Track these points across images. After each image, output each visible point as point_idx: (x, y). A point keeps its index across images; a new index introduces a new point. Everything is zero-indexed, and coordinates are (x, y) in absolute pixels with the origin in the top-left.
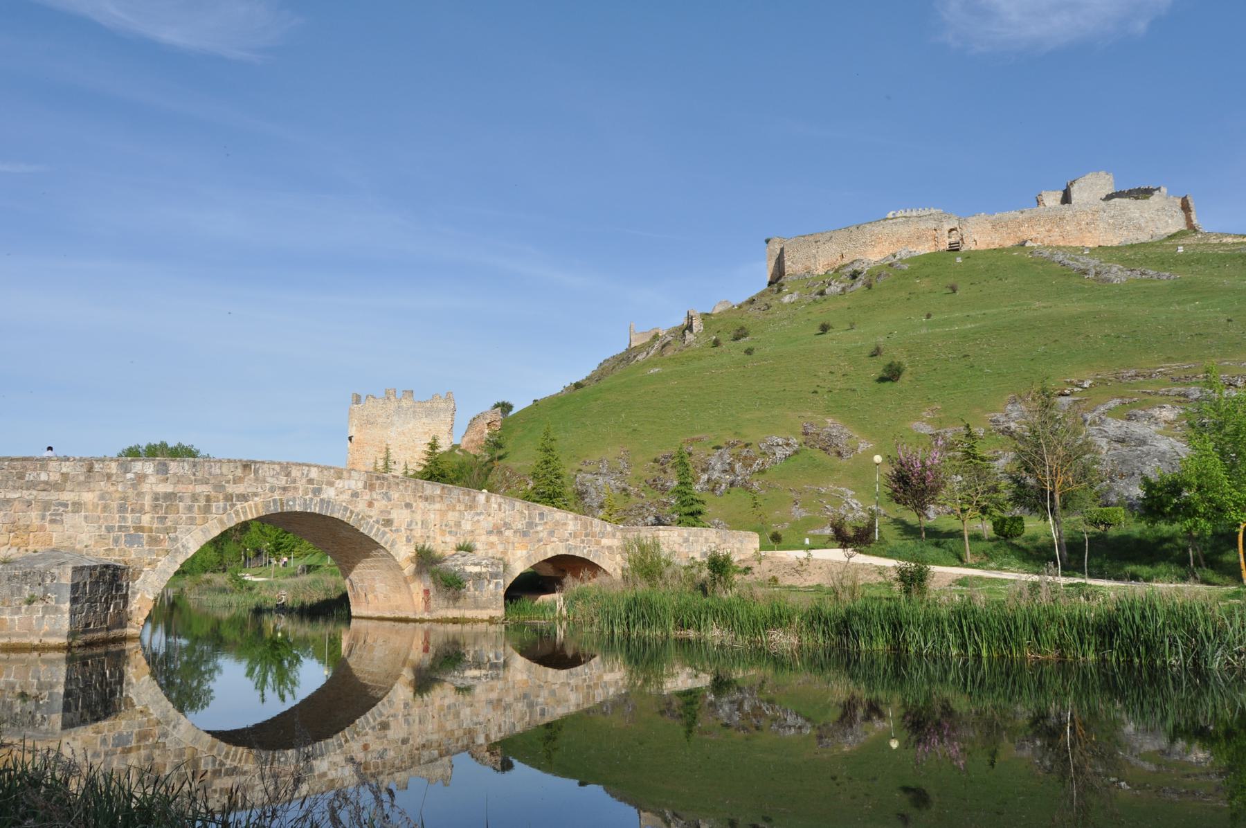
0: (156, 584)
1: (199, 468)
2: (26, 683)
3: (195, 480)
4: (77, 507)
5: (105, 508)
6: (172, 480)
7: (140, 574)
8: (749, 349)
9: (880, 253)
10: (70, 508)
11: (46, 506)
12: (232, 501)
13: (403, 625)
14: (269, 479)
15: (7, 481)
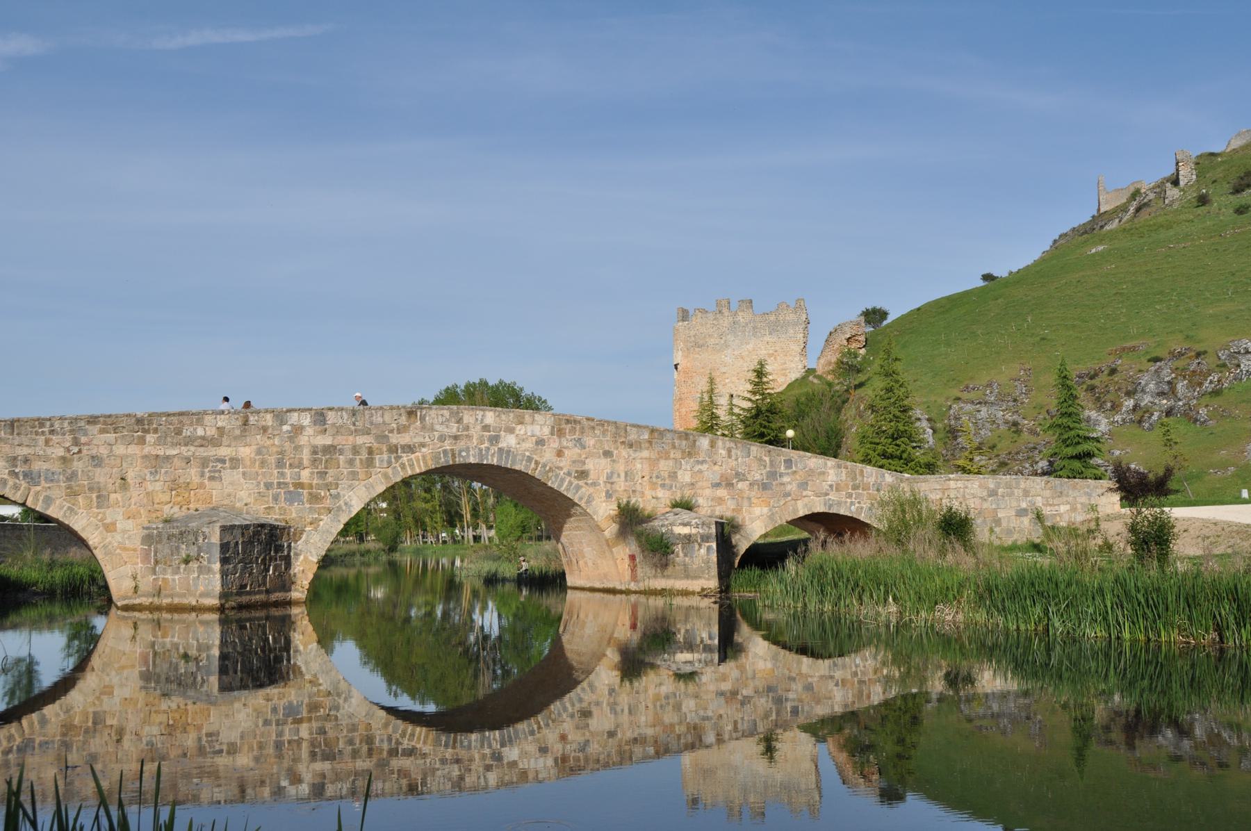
0: (319, 545)
3: (356, 430)
4: (235, 462)
5: (263, 463)
7: (301, 534)
8: (1241, 206)
10: (227, 465)
11: (204, 462)
13: (611, 597)
14: (437, 427)
15: (165, 438)
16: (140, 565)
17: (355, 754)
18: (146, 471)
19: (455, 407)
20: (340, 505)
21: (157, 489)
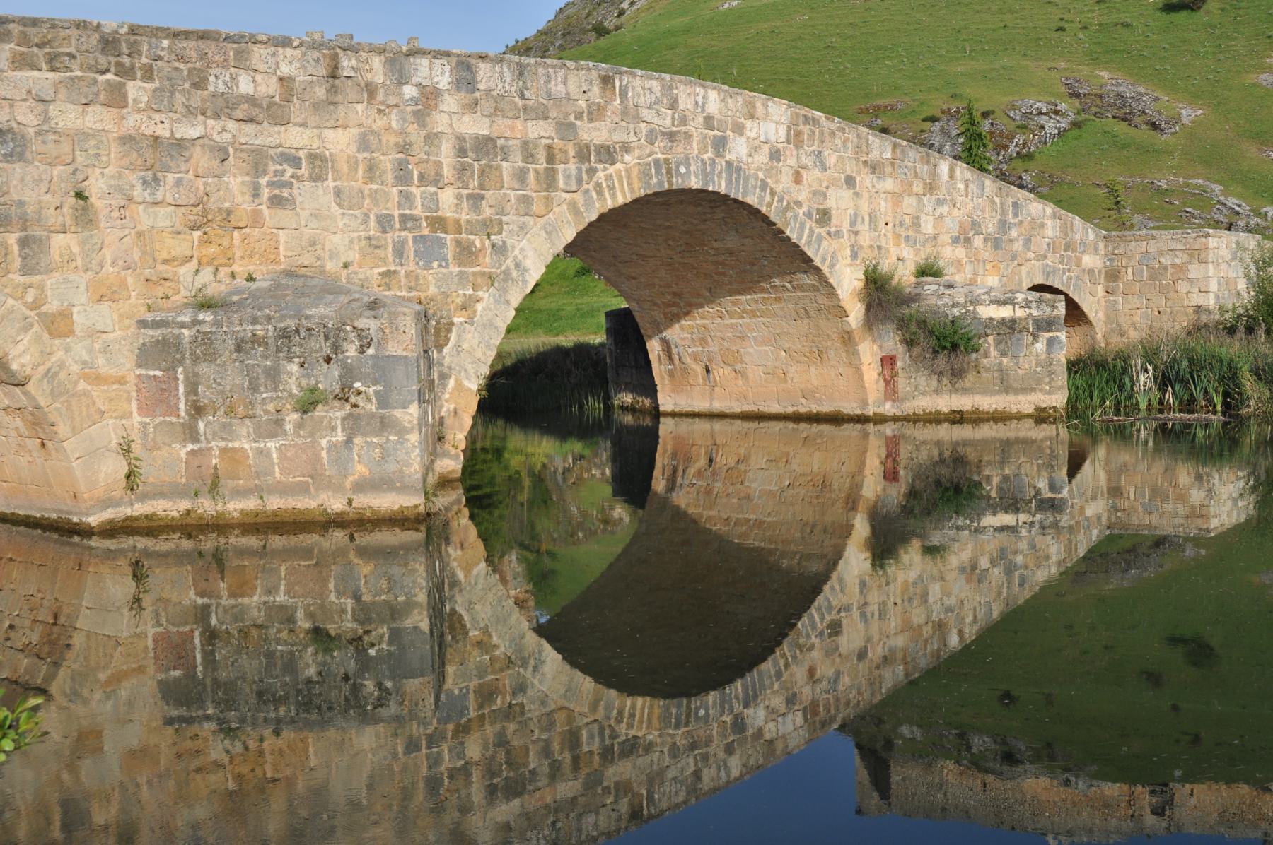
0: (479, 354)
1: (528, 78)
2: (322, 606)
3: (525, 108)
4: (319, 164)
5: (371, 168)
6: (486, 106)
7: (449, 331)
10: (304, 170)
11: (258, 161)
12: (589, 161)
13: (826, 428)
14: (646, 114)
15: (172, 93)
16: (137, 418)
17: (555, 771)
18: (133, 178)
19: (667, 77)
20: (508, 268)
21: (161, 224)
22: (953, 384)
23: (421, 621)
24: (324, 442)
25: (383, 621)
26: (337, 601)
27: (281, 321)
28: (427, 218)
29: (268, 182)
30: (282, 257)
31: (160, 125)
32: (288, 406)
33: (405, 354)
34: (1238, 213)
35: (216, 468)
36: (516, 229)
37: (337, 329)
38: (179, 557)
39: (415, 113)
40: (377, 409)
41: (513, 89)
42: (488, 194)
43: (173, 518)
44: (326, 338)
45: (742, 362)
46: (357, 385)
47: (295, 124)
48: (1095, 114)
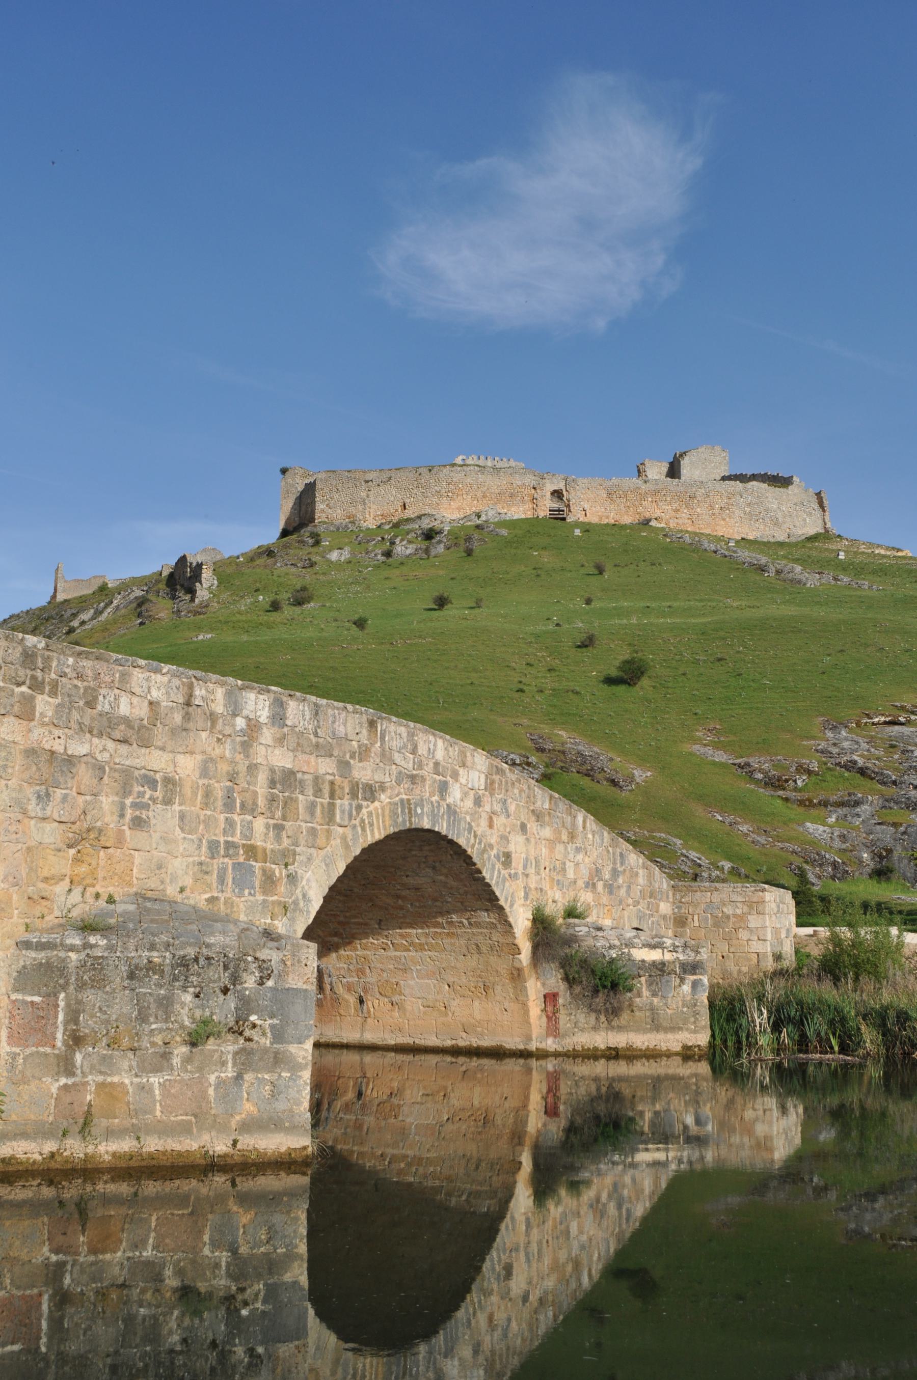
1: (321, 716)
2: (193, 1262)
5: (208, 794)
6: (292, 741)
9: (459, 509)
10: (159, 794)
13: (486, 1062)
14: (397, 757)
15: (70, 710)
19: (412, 724)
21: (48, 840)
22: (609, 1022)
23: (301, 1274)
24: (212, 1078)
25: (259, 1276)
26: (210, 1255)
27: (182, 948)
28: (244, 845)
29: (132, 803)
30: (134, 879)
31: (57, 740)
32: (178, 1039)
33: (305, 987)
34: (700, 866)
35: (90, 1105)
36: (305, 860)
37: (238, 959)
38: (35, 1207)
39: (243, 744)
40: (272, 1043)
41: (310, 727)
42: (288, 824)
43: (34, 1162)
44: (226, 967)
45: (401, 994)
46: (253, 1018)
47: (156, 748)
48: (562, 768)
